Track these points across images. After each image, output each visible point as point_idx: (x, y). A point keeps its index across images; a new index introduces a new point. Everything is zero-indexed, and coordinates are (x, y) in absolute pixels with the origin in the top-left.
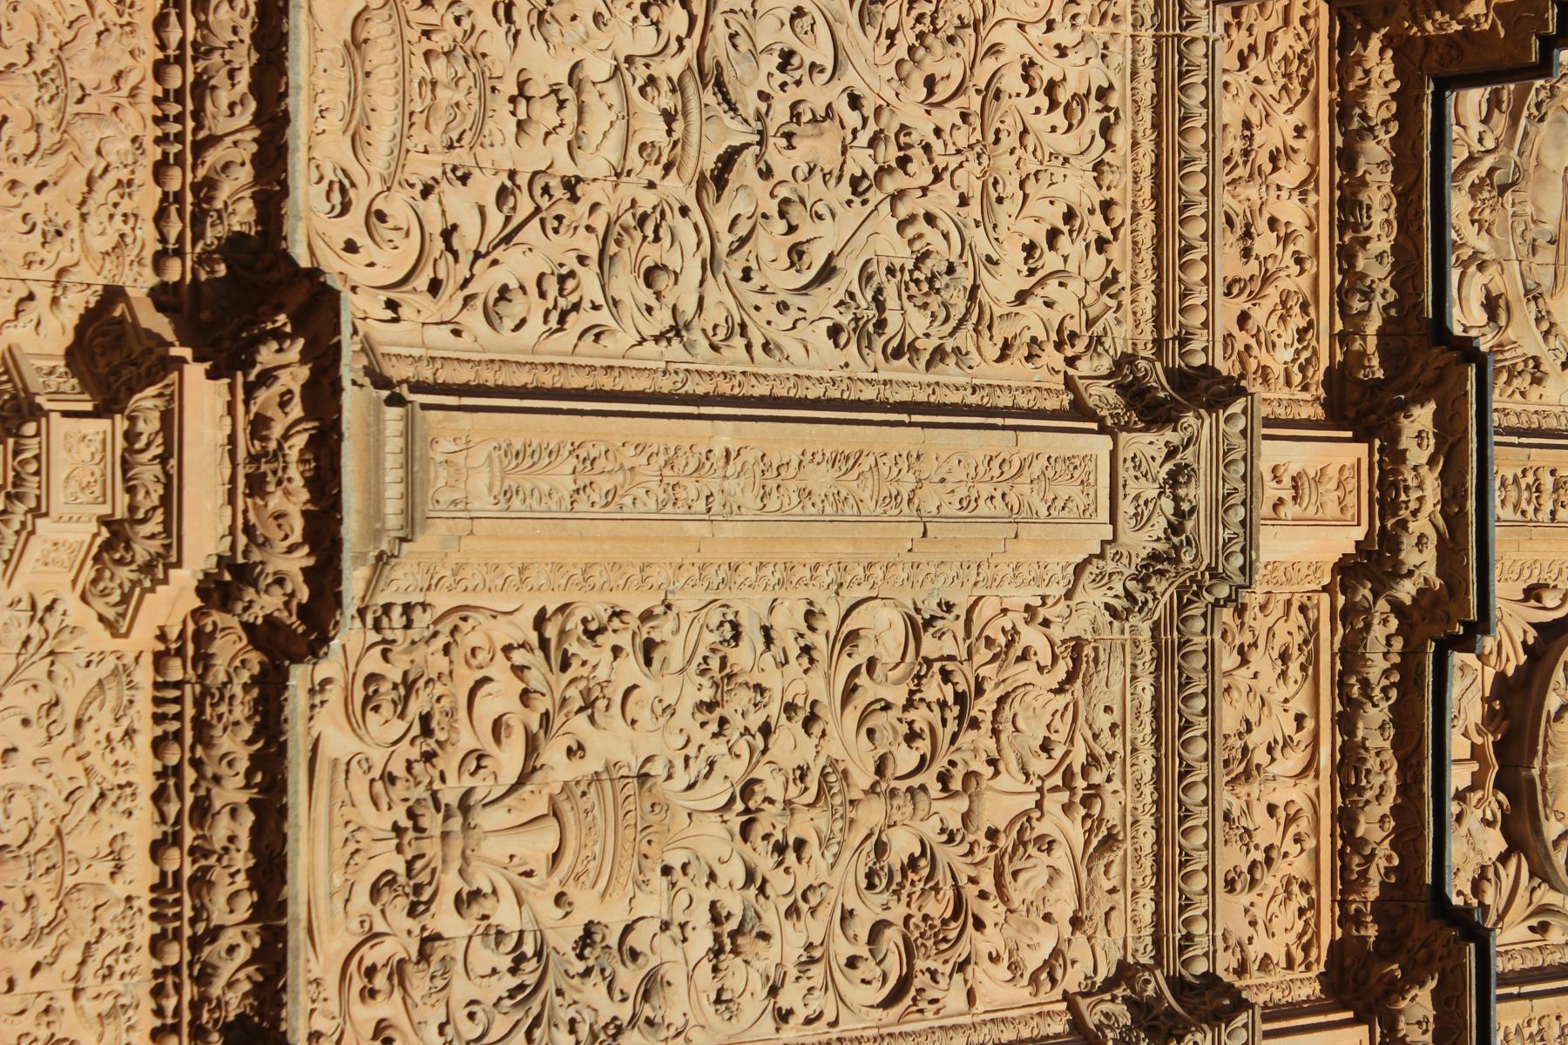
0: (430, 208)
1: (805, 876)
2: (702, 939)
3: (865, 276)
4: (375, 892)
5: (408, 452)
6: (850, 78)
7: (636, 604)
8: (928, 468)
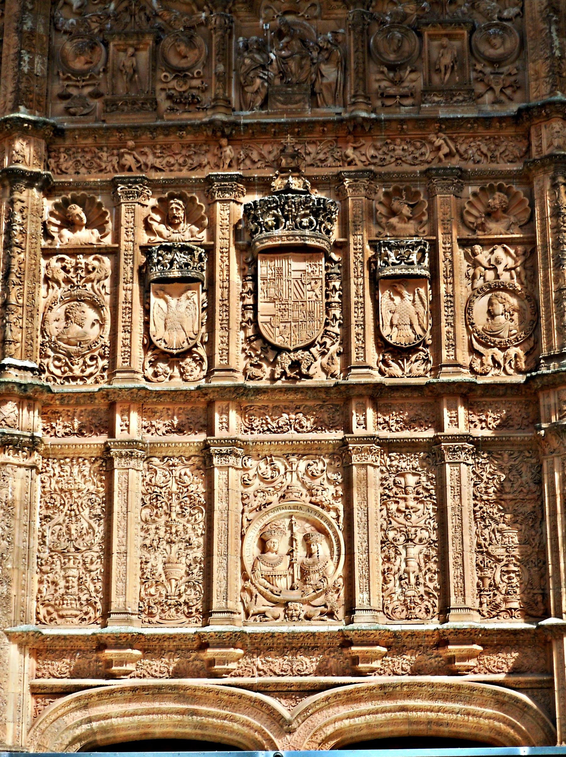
0: (84, 603)
2: (189, 551)
6: (61, 521)
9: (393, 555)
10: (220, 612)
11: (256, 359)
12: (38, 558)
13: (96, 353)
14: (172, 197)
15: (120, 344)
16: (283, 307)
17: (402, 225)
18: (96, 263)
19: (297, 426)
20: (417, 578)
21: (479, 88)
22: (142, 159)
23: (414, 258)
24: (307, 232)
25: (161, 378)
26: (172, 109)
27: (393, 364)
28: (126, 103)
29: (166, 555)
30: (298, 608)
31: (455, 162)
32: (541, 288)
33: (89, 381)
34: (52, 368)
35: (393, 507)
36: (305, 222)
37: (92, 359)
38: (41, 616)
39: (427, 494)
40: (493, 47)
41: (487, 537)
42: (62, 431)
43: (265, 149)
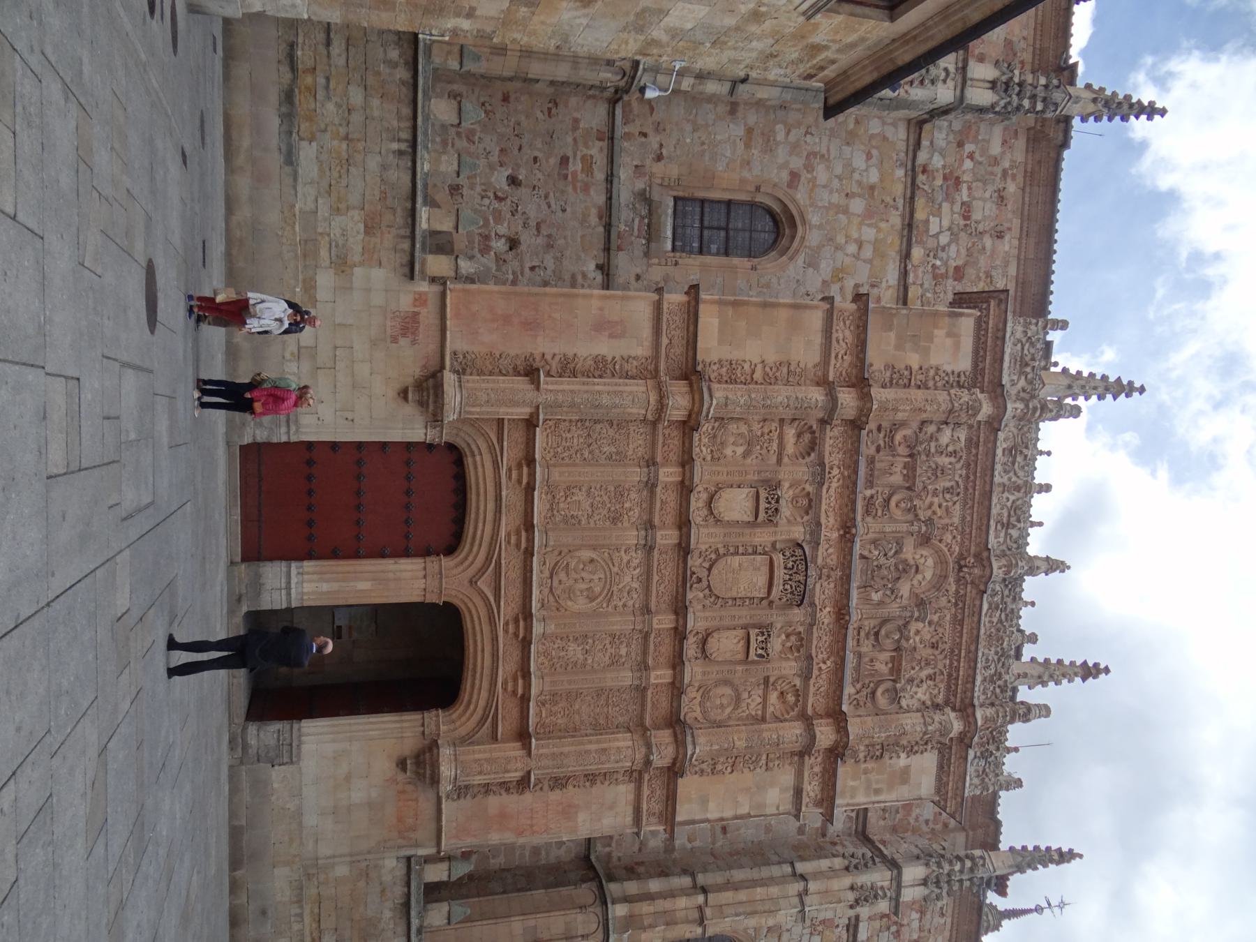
14: (810, 500)
15: (719, 468)
17: (780, 641)
21: (859, 686)
22: (835, 480)
23: (760, 652)
24: (781, 587)
26: (865, 499)
28: (871, 470)
31: (815, 672)
33: (698, 449)
35: (607, 642)
37: (712, 451)
40: (883, 693)
42: (667, 432)
43: (834, 557)
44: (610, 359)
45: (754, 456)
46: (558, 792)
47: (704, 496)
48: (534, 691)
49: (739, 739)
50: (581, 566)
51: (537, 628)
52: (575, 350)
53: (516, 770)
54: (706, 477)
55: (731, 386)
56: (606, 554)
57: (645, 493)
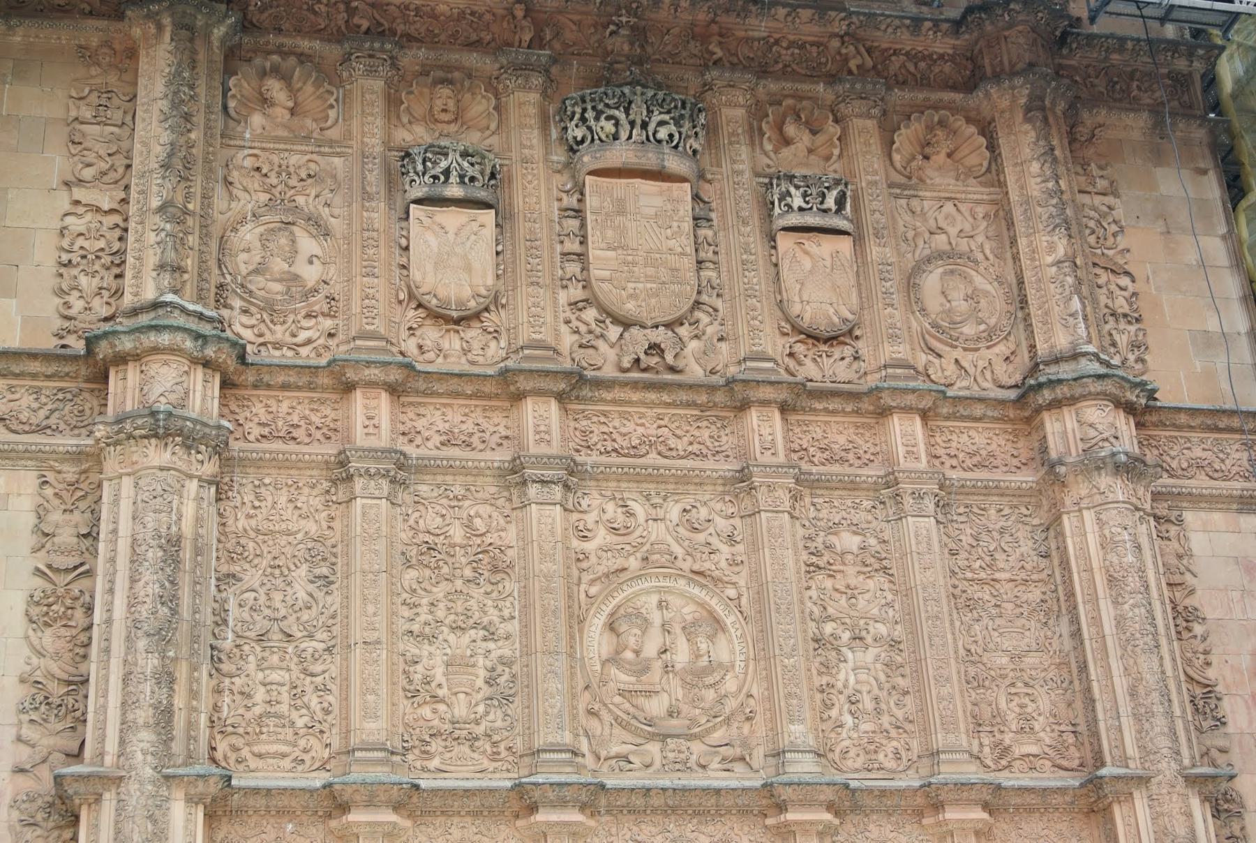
0: (302, 732)
1: (475, 608)
2: (491, 645)
3: (312, 582)
4: (474, 751)
5: (366, 750)
6: (256, 585)
7: (402, 666)
8: (366, 567)
9: (834, 662)
10: (554, 751)
11: (590, 337)
12: (212, 648)
13: (316, 308)
15: (356, 295)
16: (630, 258)
18: (312, 165)
19: (662, 448)
20: (876, 699)
23: (830, 202)
25: (431, 355)
27: (808, 361)
29: (448, 651)
30: (684, 748)
32: (1025, 262)
33: (304, 351)
34: (238, 328)
35: (828, 583)
36: (663, 134)
37: (308, 316)
38: (219, 755)
39: (876, 566)
41: (979, 638)
42: (256, 431)
44: (39, 582)
45: (325, 212)
46: (1226, 704)
47: (431, 334)
48: (972, 772)
49: (1051, 248)
50: (629, 655)
51: (803, 767)
52: (11, 681)
53: (1189, 815)
54: (379, 326)
55: (130, 260)
56: (593, 590)
57: (424, 489)
